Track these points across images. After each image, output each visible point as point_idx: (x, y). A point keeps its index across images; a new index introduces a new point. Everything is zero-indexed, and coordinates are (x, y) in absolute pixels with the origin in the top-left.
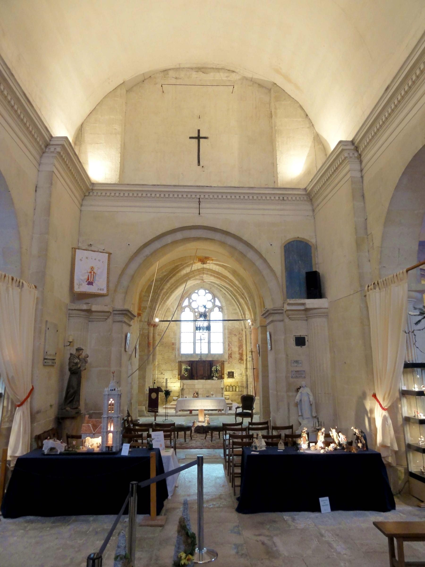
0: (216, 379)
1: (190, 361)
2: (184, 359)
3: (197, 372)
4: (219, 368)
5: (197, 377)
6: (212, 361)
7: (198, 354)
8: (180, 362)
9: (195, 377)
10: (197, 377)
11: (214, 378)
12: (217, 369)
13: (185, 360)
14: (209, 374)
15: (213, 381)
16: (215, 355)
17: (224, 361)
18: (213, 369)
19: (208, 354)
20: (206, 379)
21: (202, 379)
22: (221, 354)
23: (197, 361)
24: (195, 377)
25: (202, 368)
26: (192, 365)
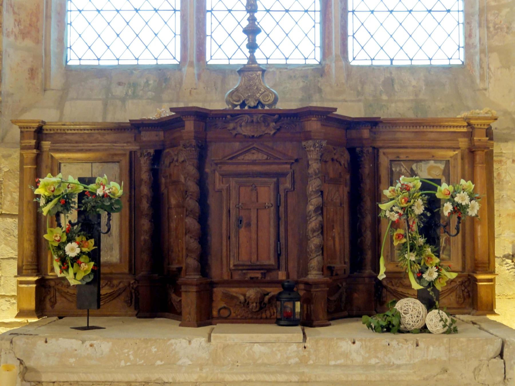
0: (434, 319)
1: (138, 127)
2: (83, 111)
3: (203, 238)
4: (458, 193)
5: (206, 290)
6: (373, 123)
7: (222, 72)
8: (40, 132)
9: (189, 300)
10: (206, 290)
11: (409, 309)
12: (433, 204)
13: (100, 120)
14: (341, 265)
15: (398, 349)
16: (390, 77)
17: (489, 133)
18: (388, 210)
19: (320, 71)
20: (307, 321)
21: (267, 311)
22: (449, 69)
23: (202, 116)
24: (189, 300)
25: (266, 194)
26: (157, 157)
